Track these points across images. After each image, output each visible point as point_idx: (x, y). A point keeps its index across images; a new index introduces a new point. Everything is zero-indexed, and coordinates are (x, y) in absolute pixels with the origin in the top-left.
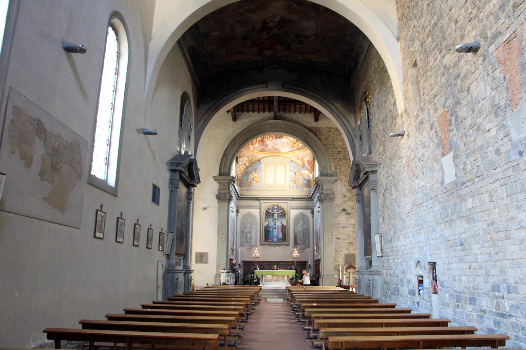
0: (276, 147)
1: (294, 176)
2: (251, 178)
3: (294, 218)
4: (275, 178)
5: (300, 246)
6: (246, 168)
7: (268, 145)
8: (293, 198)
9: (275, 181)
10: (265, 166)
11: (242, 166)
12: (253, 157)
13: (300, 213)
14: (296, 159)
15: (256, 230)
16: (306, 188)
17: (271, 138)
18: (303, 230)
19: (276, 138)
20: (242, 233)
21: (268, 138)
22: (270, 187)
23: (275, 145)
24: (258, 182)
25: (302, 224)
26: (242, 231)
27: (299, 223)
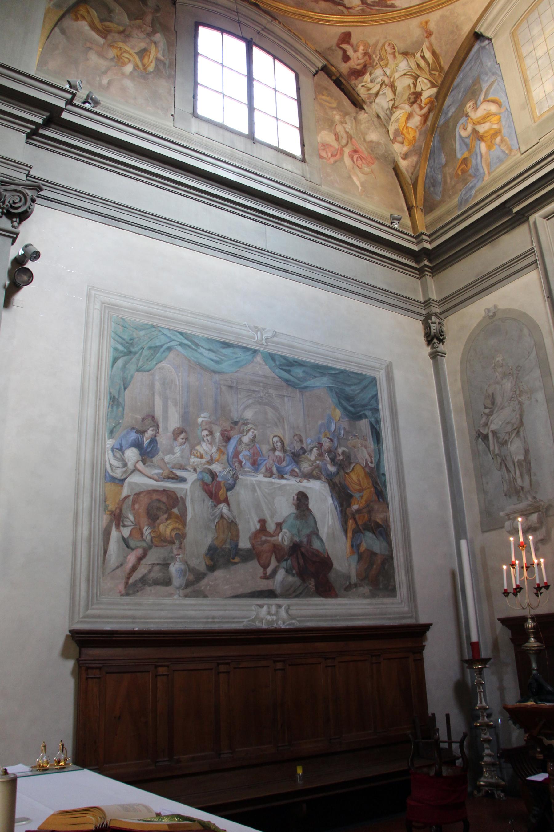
2: (460, 136)
6: (430, 111)
11: (400, 114)
12: (432, 39)
20: (481, 446)
24: (497, 132)
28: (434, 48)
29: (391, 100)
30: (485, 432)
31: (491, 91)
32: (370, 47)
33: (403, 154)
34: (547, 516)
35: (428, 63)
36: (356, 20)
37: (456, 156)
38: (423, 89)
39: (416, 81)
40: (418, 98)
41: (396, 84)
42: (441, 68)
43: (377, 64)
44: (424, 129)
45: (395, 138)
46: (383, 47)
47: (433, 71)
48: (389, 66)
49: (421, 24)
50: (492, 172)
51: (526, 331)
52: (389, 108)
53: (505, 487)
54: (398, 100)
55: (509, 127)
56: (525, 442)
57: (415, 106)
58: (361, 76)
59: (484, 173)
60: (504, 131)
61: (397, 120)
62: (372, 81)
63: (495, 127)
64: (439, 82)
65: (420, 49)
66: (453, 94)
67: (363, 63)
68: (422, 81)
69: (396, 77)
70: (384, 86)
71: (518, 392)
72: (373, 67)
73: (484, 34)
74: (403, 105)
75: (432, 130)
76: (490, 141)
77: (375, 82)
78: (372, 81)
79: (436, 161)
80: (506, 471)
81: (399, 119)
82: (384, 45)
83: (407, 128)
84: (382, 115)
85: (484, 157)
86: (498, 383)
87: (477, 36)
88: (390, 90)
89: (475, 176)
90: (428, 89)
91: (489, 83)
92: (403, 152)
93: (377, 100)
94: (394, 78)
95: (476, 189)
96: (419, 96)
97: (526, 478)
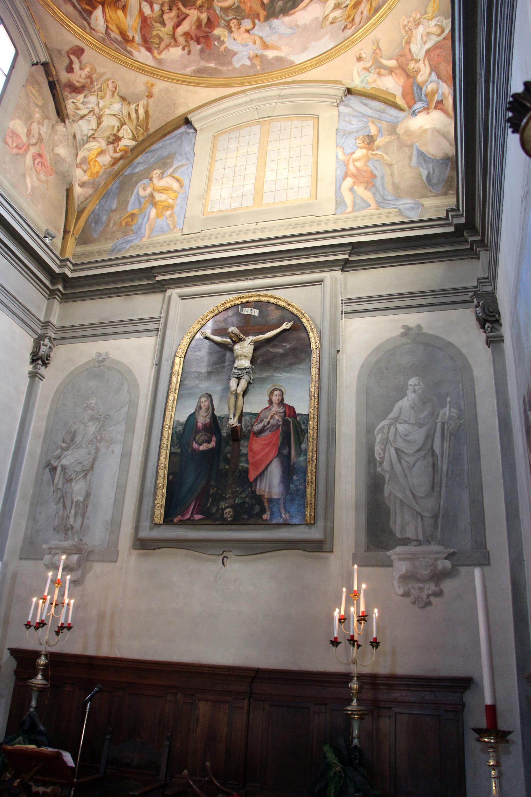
0: (270, 54)
1: (360, 153)
3: (363, 367)
4: (260, 179)
5: (412, 558)
6: (121, 158)
7: (235, 54)
8: (355, 248)
9: (258, 192)
10: (215, 138)
11: (94, 146)
12: (151, 101)
13: (407, 330)
14: (372, 77)
15: (126, 455)
16: (438, 195)
17: (247, 24)
18: (429, 437)
19: (267, 18)
20: (47, 476)
21: (233, 23)
22: (226, 218)
23: (266, 46)
24: (170, 207)
25: (424, 401)
26: (48, 464)
27: (401, 393)
28: (149, 109)
29: (93, 129)
30: (55, 464)
31: (180, 171)
32: (96, 73)
33: (81, 182)
34: (87, 560)
35: (138, 118)
36: (94, 43)
37: (126, 208)
38: (124, 137)
39: (122, 126)
40: (116, 142)
41: (103, 119)
42: (147, 129)
43: (95, 91)
44: (109, 170)
45: (81, 164)
46: (107, 81)
47: (139, 126)
48: (104, 100)
49: (148, 83)
50: (152, 237)
51: (126, 386)
52: (87, 135)
53: (56, 522)
54: (99, 133)
55: (181, 207)
56: (90, 486)
57: (111, 147)
58: (76, 93)
59: (145, 234)
60: (176, 209)
61: (89, 150)
62: (83, 103)
63: (170, 201)
64: (141, 139)
65: (136, 103)
66: (147, 155)
67: (83, 83)
68: (127, 130)
69: (106, 113)
70: (92, 114)
71: (98, 438)
72: (91, 92)
73: (193, 123)
74: (101, 140)
75: (116, 175)
76: (161, 210)
77: (86, 106)
78: (83, 103)
79: (107, 204)
80: (62, 507)
81: (91, 149)
82: (108, 80)
83: (95, 161)
84: (78, 137)
85: (150, 221)
86: (84, 423)
87: (187, 122)
88: (96, 120)
89: (136, 233)
90: (129, 139)
91: (180, 164)
92: (82, 180)
93: (81, 122)
94: (104, 112)
95: (132, 244)
96: (118, 140)
97: (79, 519)
